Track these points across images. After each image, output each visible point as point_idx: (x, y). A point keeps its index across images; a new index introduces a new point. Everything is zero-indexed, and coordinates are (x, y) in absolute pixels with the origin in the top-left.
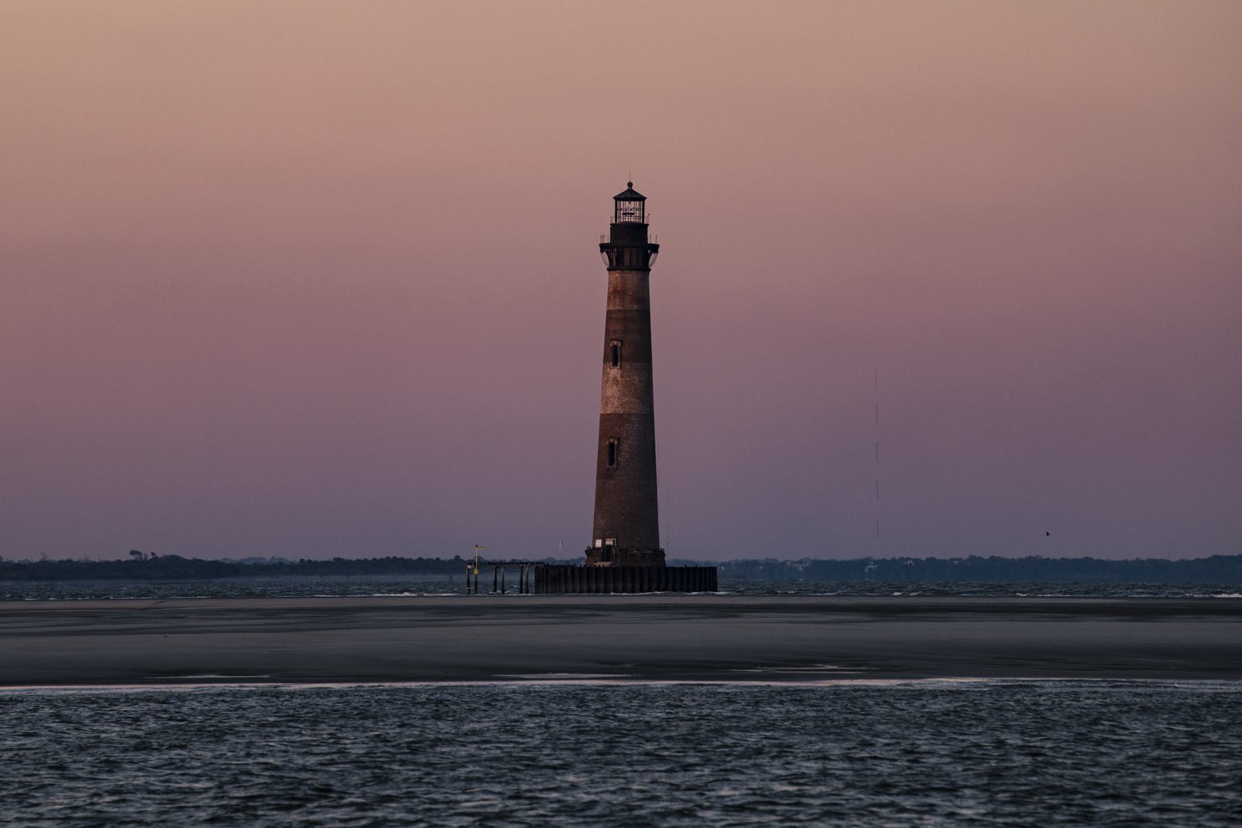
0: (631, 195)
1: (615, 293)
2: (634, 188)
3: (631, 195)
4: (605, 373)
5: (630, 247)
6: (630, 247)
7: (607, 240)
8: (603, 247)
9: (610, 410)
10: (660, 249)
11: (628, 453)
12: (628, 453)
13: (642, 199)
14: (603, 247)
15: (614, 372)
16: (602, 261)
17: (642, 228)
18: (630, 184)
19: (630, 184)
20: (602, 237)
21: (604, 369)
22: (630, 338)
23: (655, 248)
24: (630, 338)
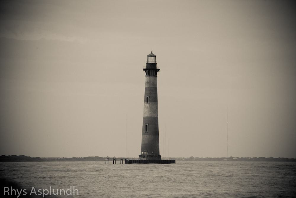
0: (152, 55)
1: (148, 83)
2: (153, 53)
3: (152, 55)
4: (144, 105)
5: (152, 70)
6: (152, 70)
7: (145, 68)
8: (144, 70)
9: (146, 116)
10: (160, 70)
11: (151, 127)
12: (151, 127)
13: (155, 56)
14: (144, 70)
15: (147, 105)
16: (144, 73)
17: (155, 64)
18: (152, 52)
19: (152, 52)
20: (144, 67)
21: (144, 104)
22: (152, 96)
23: (159, 70)
24: (152, 96)
